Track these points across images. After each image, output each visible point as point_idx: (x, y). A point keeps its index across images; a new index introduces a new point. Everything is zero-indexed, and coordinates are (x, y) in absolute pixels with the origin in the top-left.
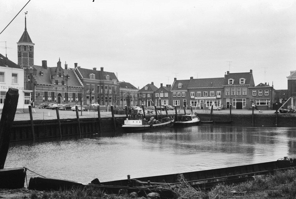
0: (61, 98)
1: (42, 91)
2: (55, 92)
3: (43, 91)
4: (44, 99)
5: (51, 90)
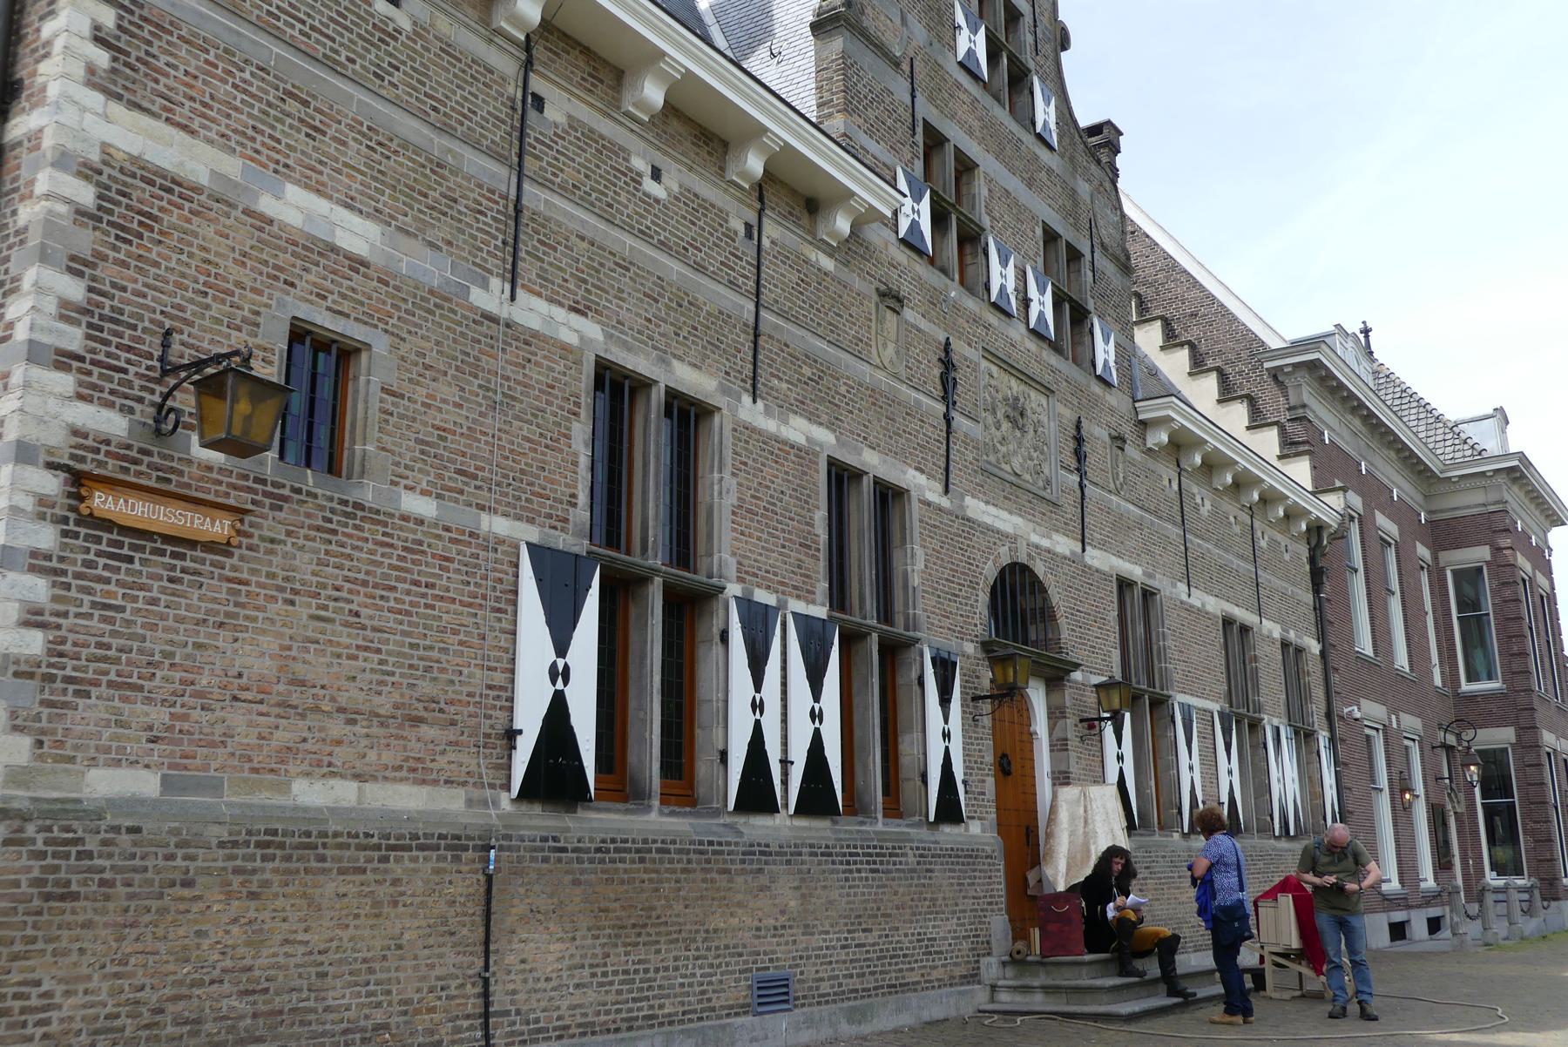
0: (1041, 725)
1: (489, 297)
2: (920, 484)
3: (532, 312)
4: (550, 669)
5: (818, 393)
